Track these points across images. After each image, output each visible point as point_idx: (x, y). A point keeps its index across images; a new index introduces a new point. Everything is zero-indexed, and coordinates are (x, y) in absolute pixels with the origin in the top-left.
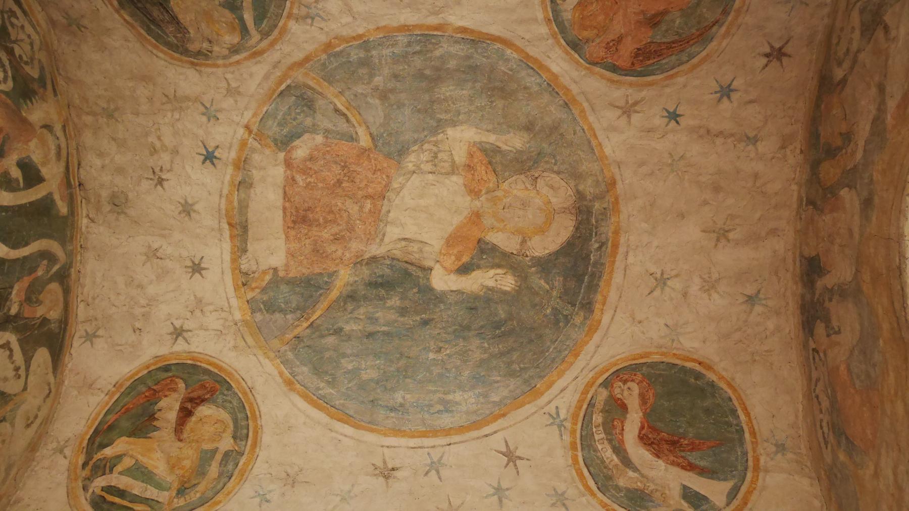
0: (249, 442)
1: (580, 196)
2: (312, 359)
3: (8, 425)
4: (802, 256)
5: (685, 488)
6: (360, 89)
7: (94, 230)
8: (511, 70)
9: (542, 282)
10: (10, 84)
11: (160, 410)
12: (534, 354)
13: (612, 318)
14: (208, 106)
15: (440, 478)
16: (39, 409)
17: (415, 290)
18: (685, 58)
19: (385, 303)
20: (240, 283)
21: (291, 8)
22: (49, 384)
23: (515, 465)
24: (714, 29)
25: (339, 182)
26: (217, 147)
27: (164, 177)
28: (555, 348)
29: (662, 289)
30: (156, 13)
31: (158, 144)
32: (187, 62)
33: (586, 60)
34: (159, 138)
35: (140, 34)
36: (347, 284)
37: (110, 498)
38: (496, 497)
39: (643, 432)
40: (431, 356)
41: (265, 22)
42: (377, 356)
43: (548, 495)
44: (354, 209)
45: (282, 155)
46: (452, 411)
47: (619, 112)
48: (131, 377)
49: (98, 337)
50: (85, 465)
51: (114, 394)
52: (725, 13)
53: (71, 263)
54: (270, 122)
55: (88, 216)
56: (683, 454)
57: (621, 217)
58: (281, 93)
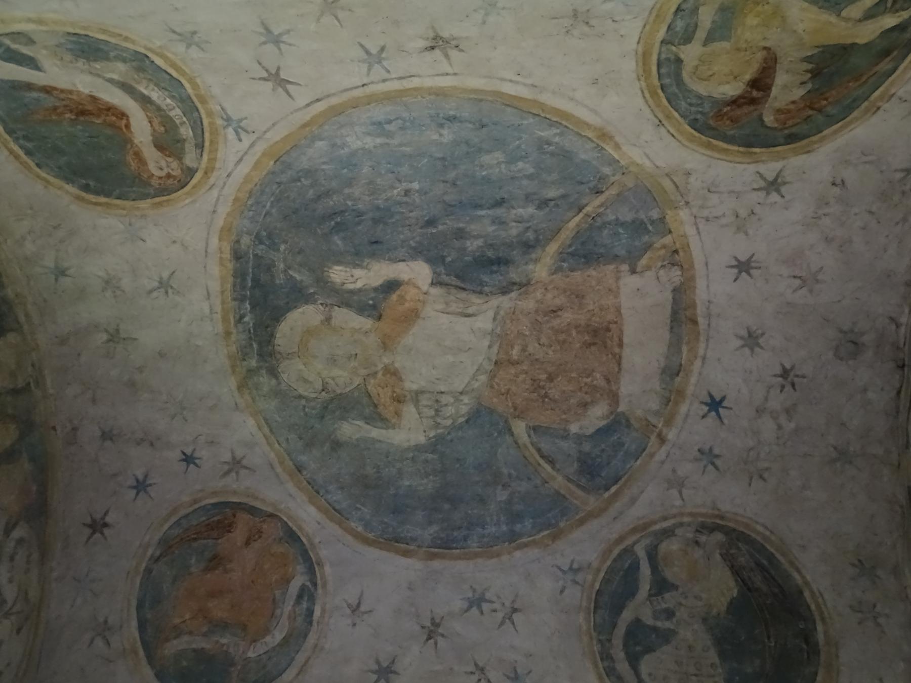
0: (654, 58)
1: (273, 373)
2: (572, 168)
9: (298, 277)
11: (803, 83)
12: (288, 197)
13: (207, 244)
14: (710, 467)
15: (362, 46)
17: (449, 259)
20: (681, 253)
21: (594, 581)
23: (267, 71)
24: (158, 553)
25: (551, 378)
26: (703, 417)
27: (780, 379)
28: (264, 206)
29: (161, 278)
30: (757, 580)
31: (783, 420)
33: (281, 519)
34: (780, 427)
36: (537, 261)
38: (276, 33)
40: (416, 186)
41: (627, 565)
42: (487, 180)
43: (207, 42)
44: (533, 347)
45: (621, 409)
46: (374, 124)
47: (244, 462)
48: (850, 123)
49: (902, 170)
51: (881, 98)
52: (148, 571)
54: (634, 447)
55: (898, 326)
56: (64, 103)
57: (226, 351)
58: (616, 482)
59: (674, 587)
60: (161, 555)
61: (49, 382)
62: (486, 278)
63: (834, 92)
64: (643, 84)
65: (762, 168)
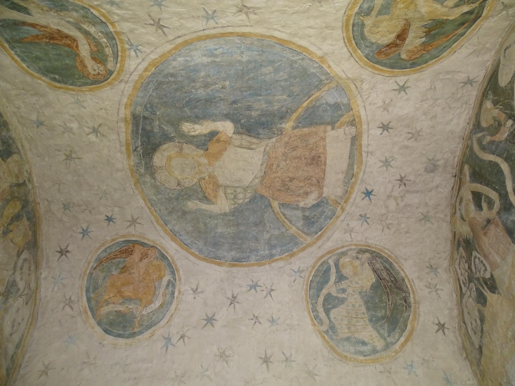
0: (351, 22)
1: (152, 175)
2: (308, 77)
4: (19, 153)
5: (29, 14)
7: (451, 152)
8: (195, 243)
10: (474, 253)
14: (365, 223)
15: (204, 9)
18: (108, 250)
19: (262, 112)
21: (309, 276)
22: (504, 56)
24: (95, 265)
28: (149, 92)
30: (384, 274)
32: (373, 247)
35: (397, 263)
39: (75, 44)
41: (325, 269)
48: (442, 58)
49: (462, 83)
52: (91, 274)
53: (471, 132)
54: (329, 213)
56: (43, 33)
59: (347, 279)
60: (97, 266)
61: (35, 180)
63: (435, 43)
64: (345, 34)
65: (398, 79)
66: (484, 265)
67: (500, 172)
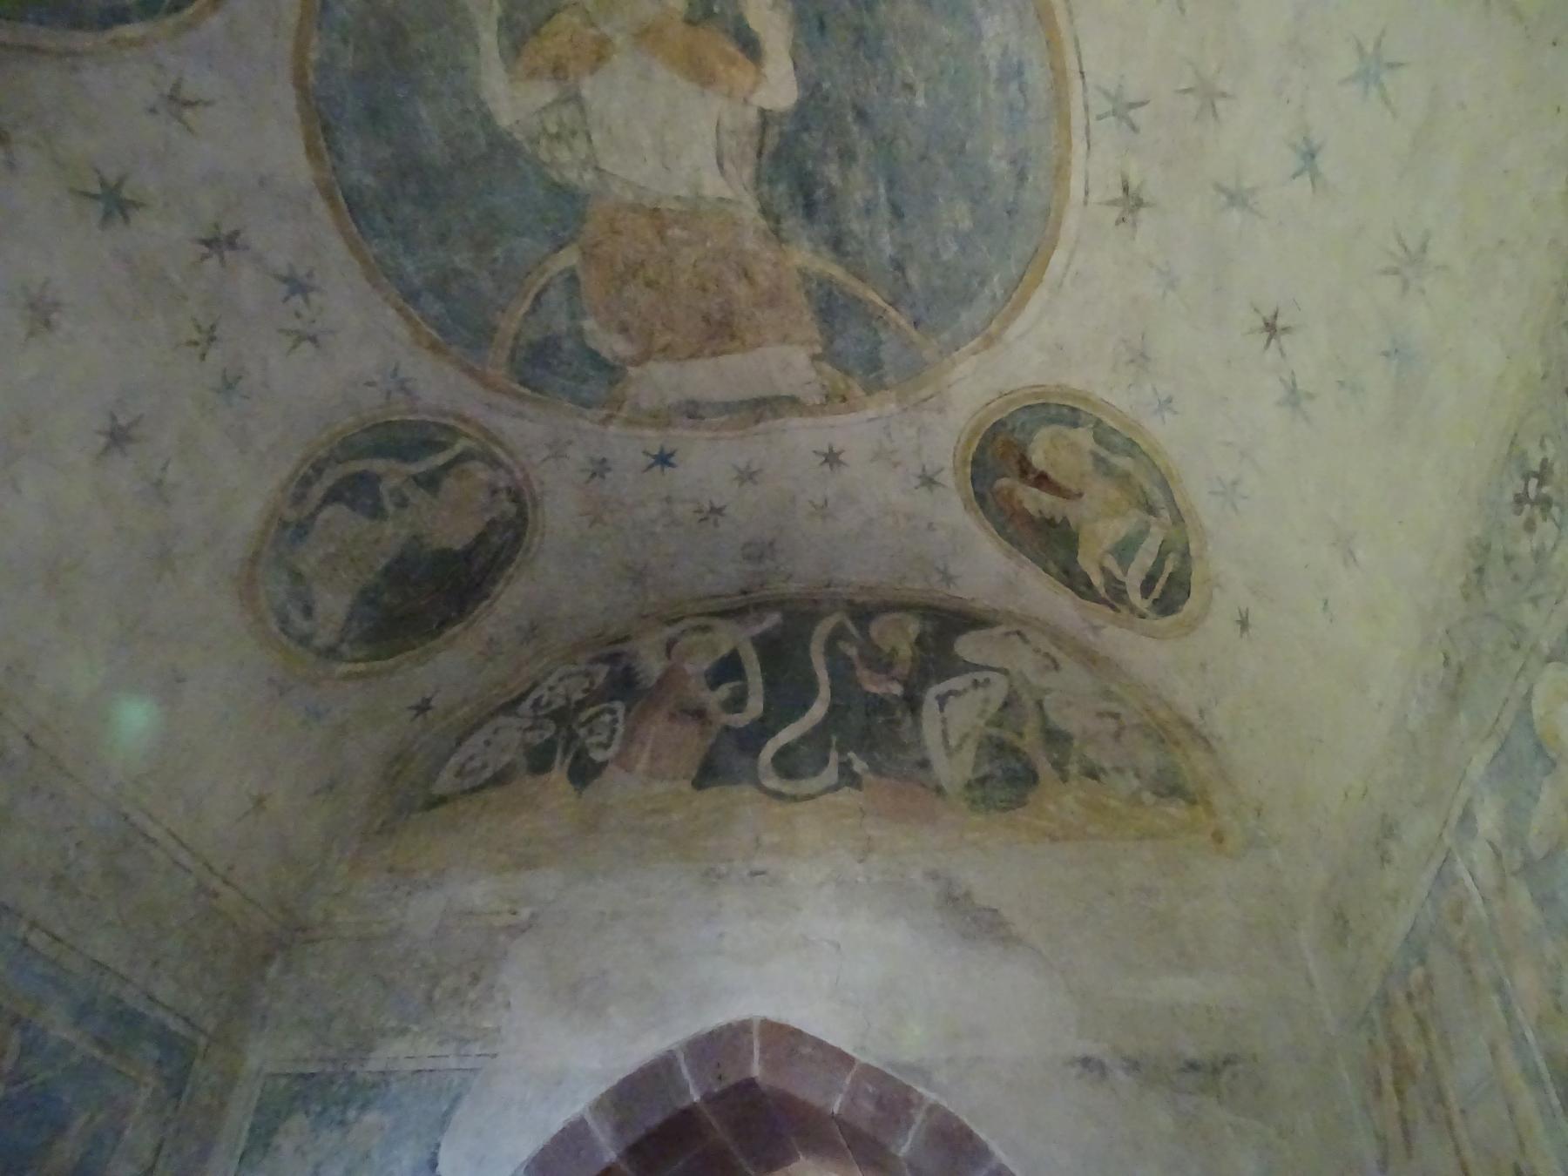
0: (1082, 407)
2: (950, 302)
3: (1048, 697)
6: (486, 284)
10: (619, 706)
15: (1143, 104)
16: (1037, 651)
17: (805, 137)
22: (1007, 634)
25: (649, 284)
26: (646, 453)
36: (816, 252)
37: (1156, 594)
45: (633, 371)
46: (1020, 64)
50: (1112, 607)
58: (534, 390)
62: (782, 188)
66: (611, 738)
67: (806, 707)
